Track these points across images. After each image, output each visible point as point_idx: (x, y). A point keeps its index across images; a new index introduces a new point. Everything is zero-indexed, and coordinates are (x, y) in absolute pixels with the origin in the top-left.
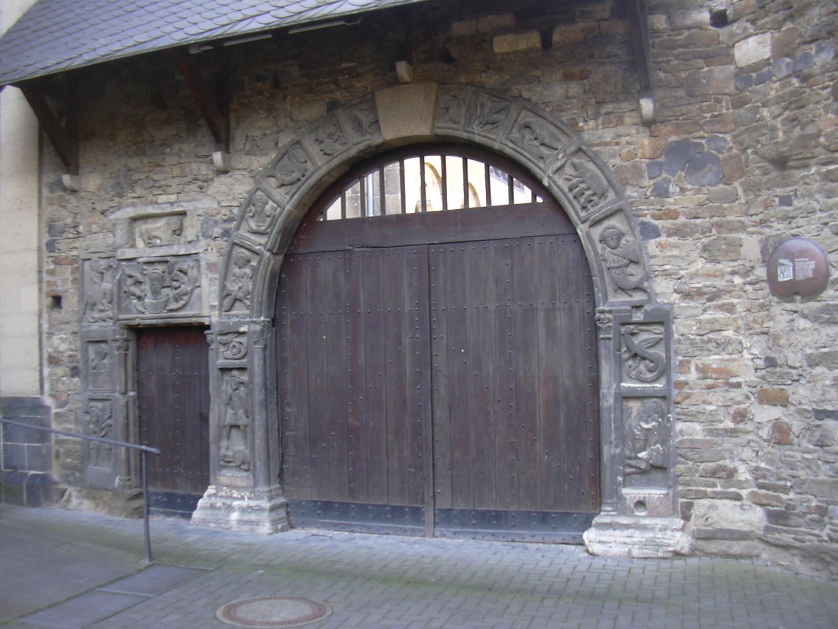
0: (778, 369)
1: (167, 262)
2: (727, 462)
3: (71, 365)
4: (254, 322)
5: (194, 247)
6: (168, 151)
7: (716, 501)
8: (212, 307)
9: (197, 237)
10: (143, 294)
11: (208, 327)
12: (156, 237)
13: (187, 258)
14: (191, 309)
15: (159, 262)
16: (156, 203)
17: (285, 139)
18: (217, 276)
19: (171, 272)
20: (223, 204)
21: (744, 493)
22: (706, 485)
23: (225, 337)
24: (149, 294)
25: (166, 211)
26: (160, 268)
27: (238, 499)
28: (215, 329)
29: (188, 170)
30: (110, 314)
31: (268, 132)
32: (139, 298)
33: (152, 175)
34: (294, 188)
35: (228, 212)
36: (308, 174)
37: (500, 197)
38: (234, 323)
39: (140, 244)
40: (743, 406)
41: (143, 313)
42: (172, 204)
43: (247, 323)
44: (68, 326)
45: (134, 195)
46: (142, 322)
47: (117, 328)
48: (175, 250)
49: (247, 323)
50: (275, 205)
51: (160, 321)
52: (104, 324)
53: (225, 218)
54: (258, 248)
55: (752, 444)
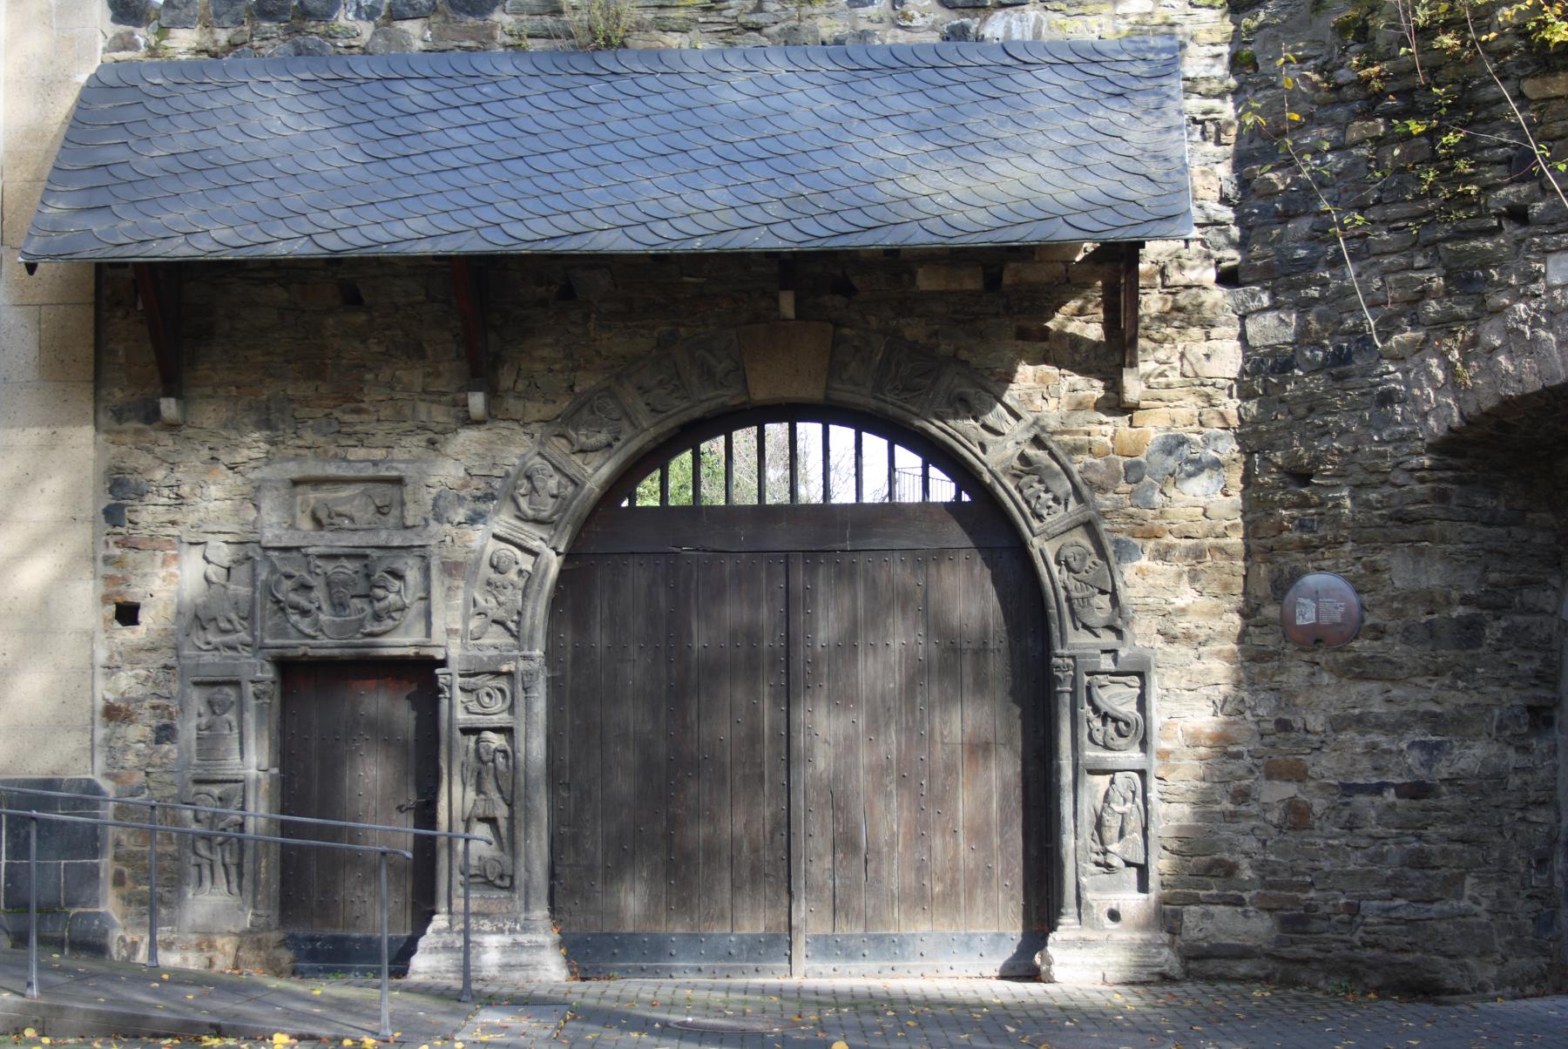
0: (1293, 735)
1: (366, 556)
2: (1226, 856)
3: (154, 723)
4: (525, 658)
6: (369, 376)
7: (1212, 908)
8: (450, 632)
9: (426, 520)
10: (313, 607)
11: (443, 663)
14: (407, 633)
15: (348, 556)
16: (345, 459)
17: (586, 382)
20: (474, 472)
21: (1246, 896)
22: (1198, 887)
23: (472, 680)
25: (363, 474)
26: (350, 566)
27: (492, 933)
28: (455, 667)
29: (407, 411)
30: (244, 636)
31: (557, 367)
32: (305, 613)
33: (337, 413)
35: (482, 485)
36: (623, 438)
37: (909, 492)
38: (490, 658)
39: (306, 524)
40: (1246, 782)
42: (375, 463)
43: (515, 658)
44: (154, 655)
45: (301, 443)
46: (311, 652)
48: (382, 538)
49: (515, 658)
50: (564, 481)
53: (479, 493)
55: (1257, 832)
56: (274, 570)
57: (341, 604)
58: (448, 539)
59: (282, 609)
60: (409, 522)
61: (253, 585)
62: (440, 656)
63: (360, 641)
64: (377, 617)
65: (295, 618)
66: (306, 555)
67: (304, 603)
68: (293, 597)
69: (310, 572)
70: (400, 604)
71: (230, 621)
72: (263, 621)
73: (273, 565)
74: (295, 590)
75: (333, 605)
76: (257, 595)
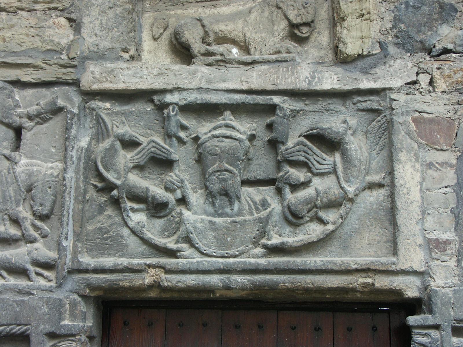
1: (272, 109)
5: (366, 72)
8: (434, 246)
9: (382, 45)
10: (170, 198)
12: (222, 40)
13: (336, 105)
14: (346, 248)
15: (237, 109)
18: (451, 157)
19: (285, 140)
24: (196, 198)
26: (244, 127)
30: (42, 250)
32: (157, 208)
41: (172, 254)
47: (66, 295)
51: (241, 280)
52: (22, 283)
56: (101, 131)
57: (225, 193)
58: (424, 79)
59: (116, 203)
60: (351, 48)
61: (65, 159)
62: (411, 288)
63: (263, 261)
64: (294, 218)
65: (138, 218)
66: (162, 107)
67: (158, 192)
68: (135, 179)
69: (169, 136)
70: (335, 192)
71: (16, 222)
72: (81, 220)
73: (99, 121)
74: (139, 168)
75: (210, 195)
76: (70, 174)
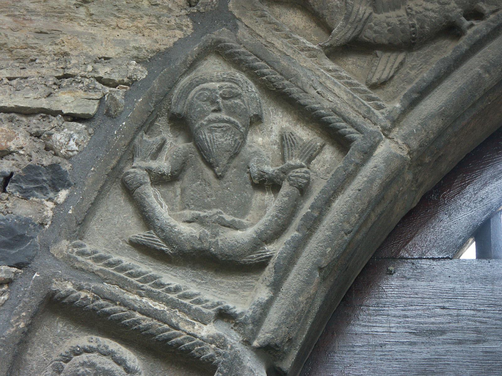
34: (420, 67)
50: (304, 134)
54: (206, 331)
